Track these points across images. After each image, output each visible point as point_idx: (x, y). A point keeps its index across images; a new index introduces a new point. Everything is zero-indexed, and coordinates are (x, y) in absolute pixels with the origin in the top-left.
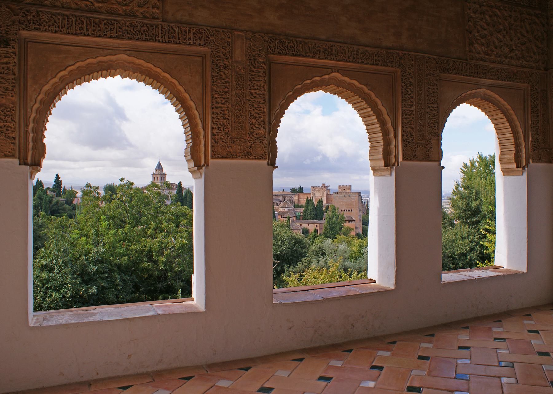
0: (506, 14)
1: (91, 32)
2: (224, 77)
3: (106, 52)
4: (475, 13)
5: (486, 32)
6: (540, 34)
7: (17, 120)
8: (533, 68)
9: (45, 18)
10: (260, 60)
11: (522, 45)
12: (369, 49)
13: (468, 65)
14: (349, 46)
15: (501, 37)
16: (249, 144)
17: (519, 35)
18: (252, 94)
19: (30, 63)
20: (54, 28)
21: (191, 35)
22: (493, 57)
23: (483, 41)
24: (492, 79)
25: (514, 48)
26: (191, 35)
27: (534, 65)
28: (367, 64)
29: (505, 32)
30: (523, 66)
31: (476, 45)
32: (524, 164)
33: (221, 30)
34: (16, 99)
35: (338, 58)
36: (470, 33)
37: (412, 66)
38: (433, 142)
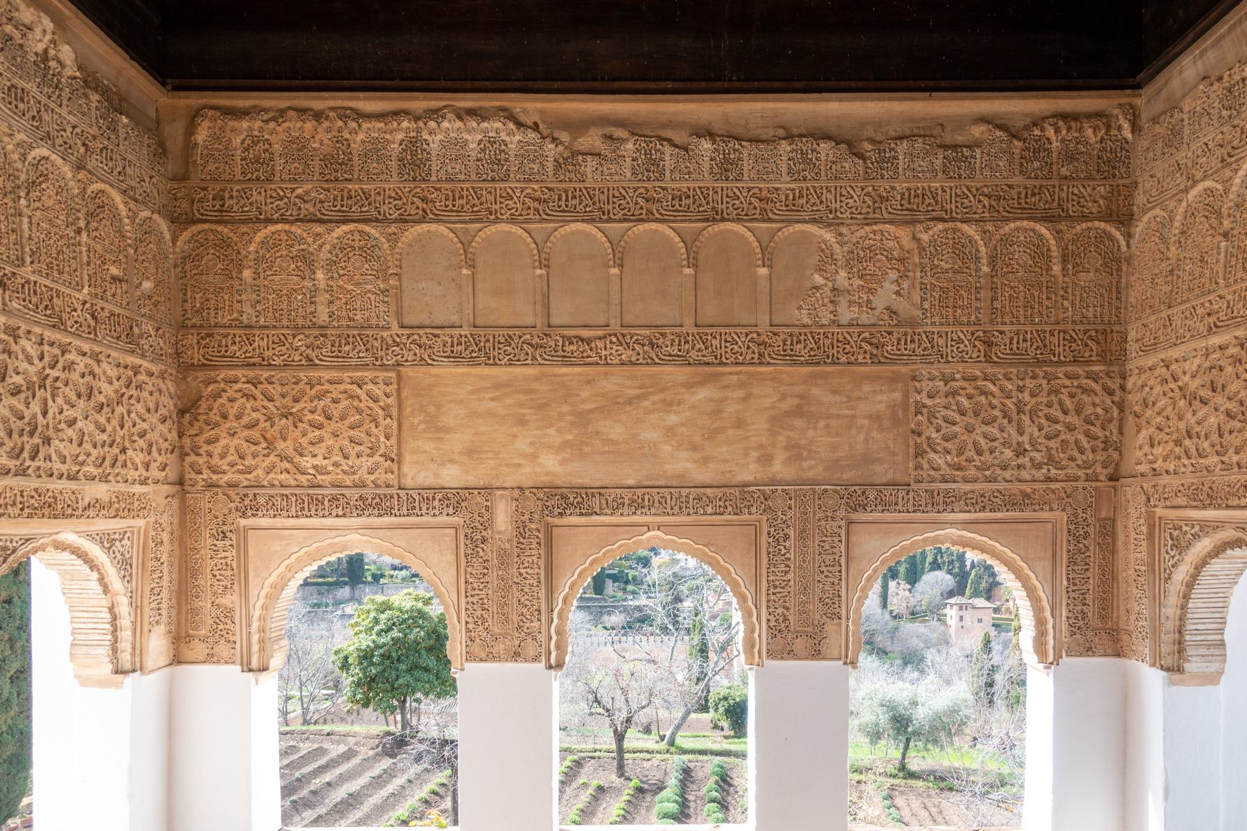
0: (1010, 387)
1: (313, 512)
2: (481, 554)
3: (334, 533)
4: (930, 397)
5: (956, 428)
6: (1099, 411)
7: (237, 621)
8: (1076, 479)
9: (262, 501)
10: (533, 526)
11: (1048, 438)
12: (709, 491)
13: (911, 494)
14: (673, 490)
15: (995, 431)
16: (517, 643)
17: (1043, 421)
18: (521, 574)
19: (250, 553)
20: (272, 513)
21: (436, 503)
22: (972, 472)
23: (949, 445)
24: (969, 511)
25: (1028, 447)
26: (436, 503)
27: (1081, 473)
28: (705, 514)
29: (1006, 421)
30: (1049, 479)
31: (932, 455)
32: (1051, 659)
33: (476, 492)
34: (235, 597)
35: (653, 511)
36: (919, 435)
37: (790, 508)
38: (830, 627)
